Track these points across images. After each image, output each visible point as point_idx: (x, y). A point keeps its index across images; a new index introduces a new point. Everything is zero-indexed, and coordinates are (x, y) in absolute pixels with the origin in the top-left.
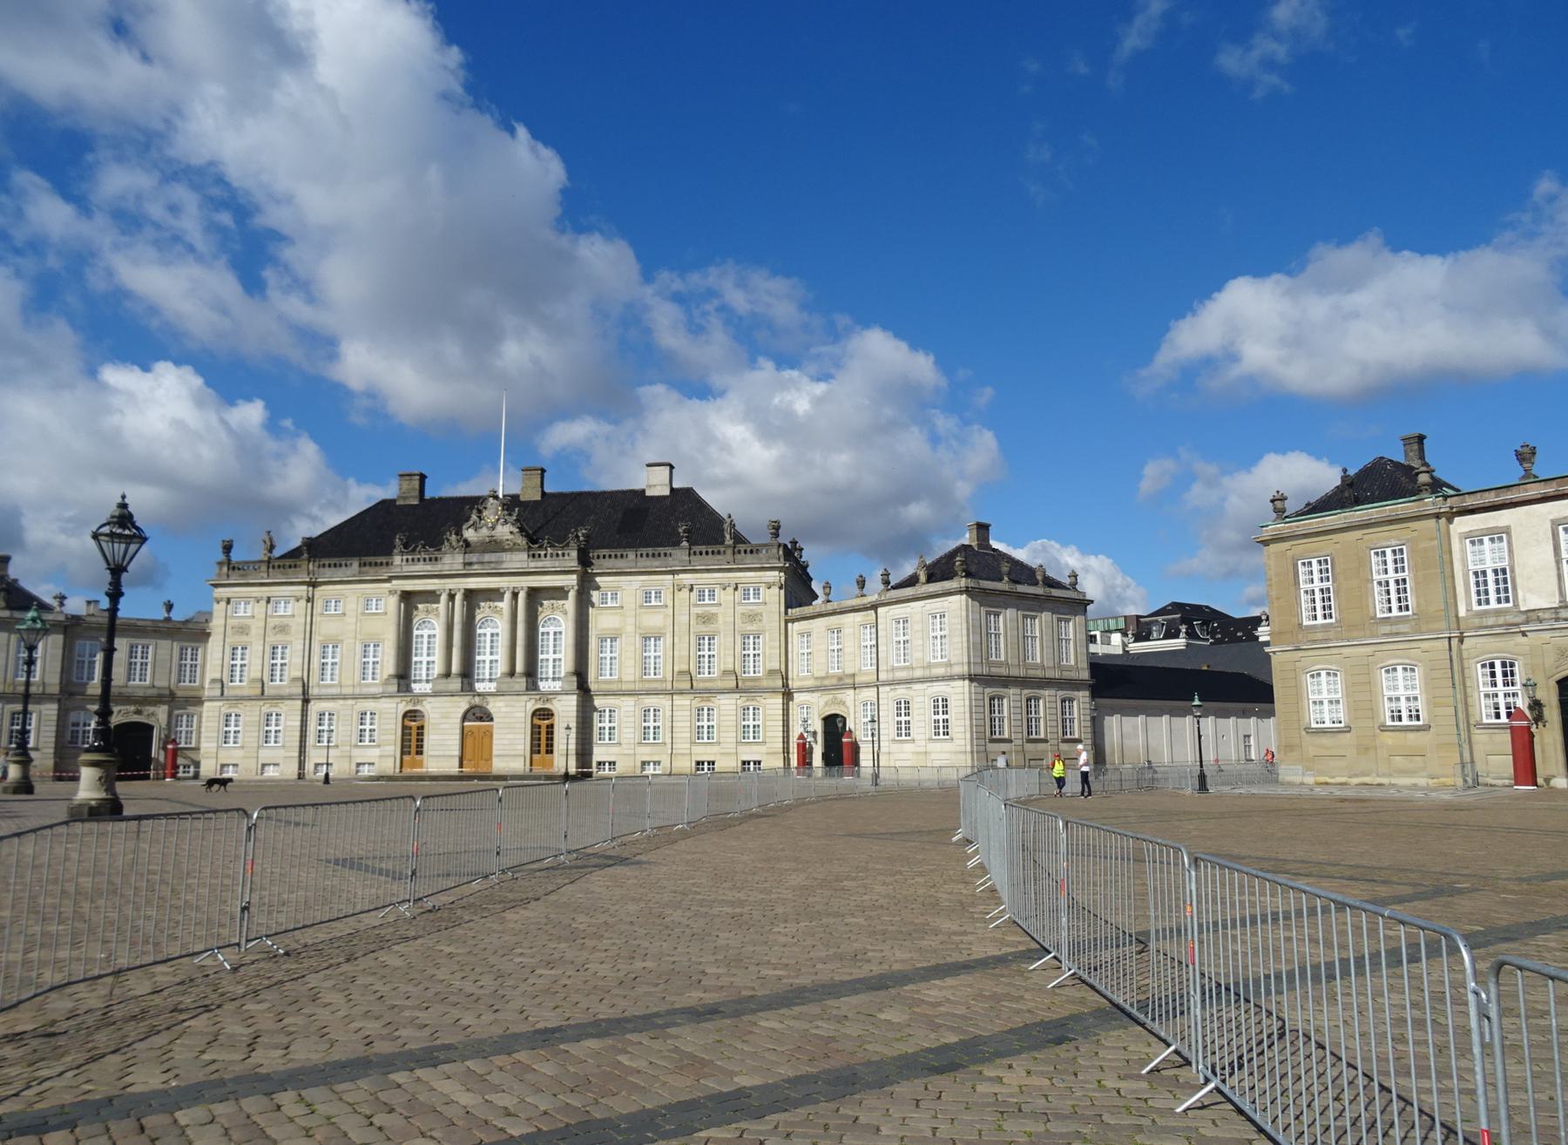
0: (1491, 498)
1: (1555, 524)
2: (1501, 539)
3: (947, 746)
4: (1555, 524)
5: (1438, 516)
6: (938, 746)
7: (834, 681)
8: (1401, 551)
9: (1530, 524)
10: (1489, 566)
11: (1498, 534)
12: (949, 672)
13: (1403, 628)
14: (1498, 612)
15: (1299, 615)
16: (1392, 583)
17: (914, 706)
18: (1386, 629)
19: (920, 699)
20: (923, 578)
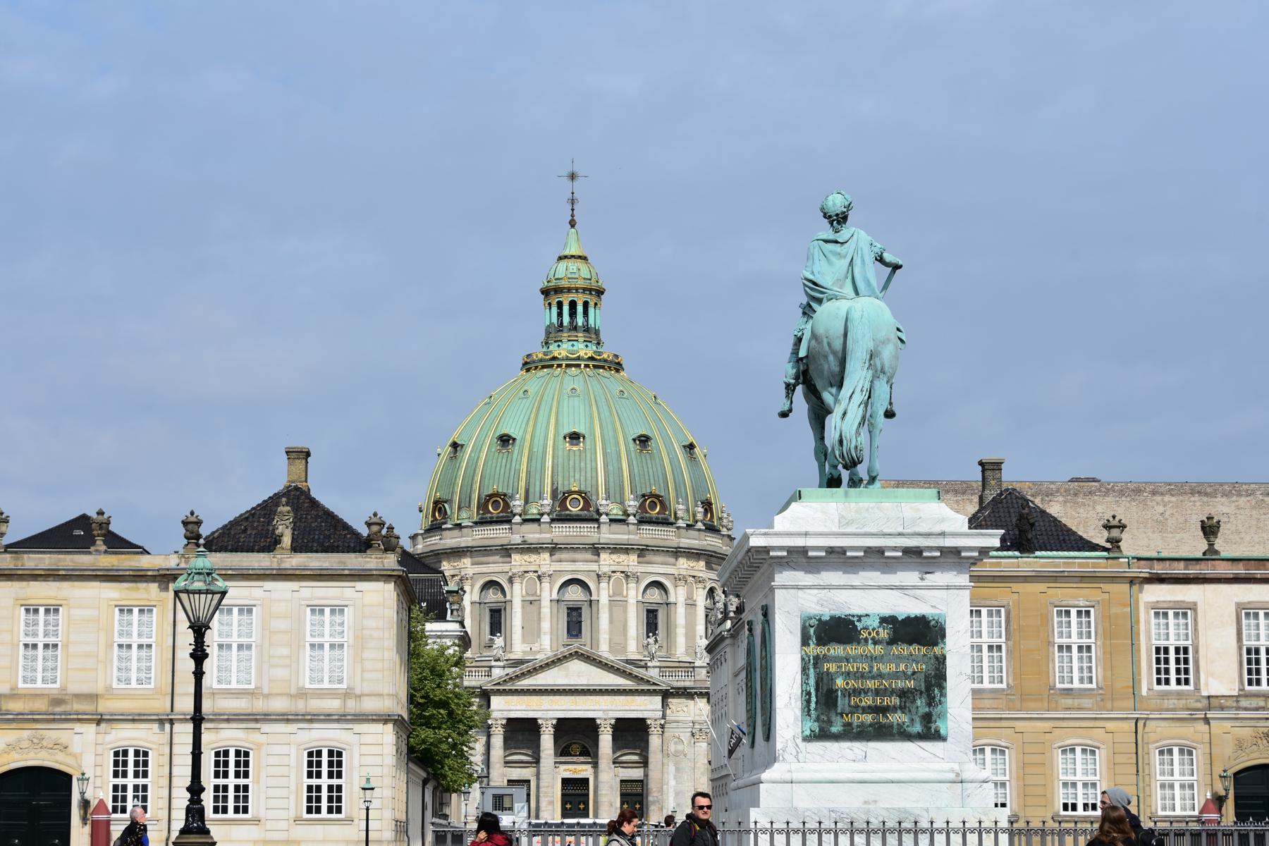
0: (1179, 569)
1: (1240, 607)
2: (1185, 615)
3: (336, 831)
4: (1240, 607)
5: (1132, 581)
6: (317, 831)
7: (41, 705)
8: (1088, 613)
9: (1217, 603)
10: (1172, 643)
11: (1185, 610)
12: (352, 706)
13: (1086, 702)
14: (1179, 695)
16: (1075, 648)
18: (1069, 702)
20: (287, 541)
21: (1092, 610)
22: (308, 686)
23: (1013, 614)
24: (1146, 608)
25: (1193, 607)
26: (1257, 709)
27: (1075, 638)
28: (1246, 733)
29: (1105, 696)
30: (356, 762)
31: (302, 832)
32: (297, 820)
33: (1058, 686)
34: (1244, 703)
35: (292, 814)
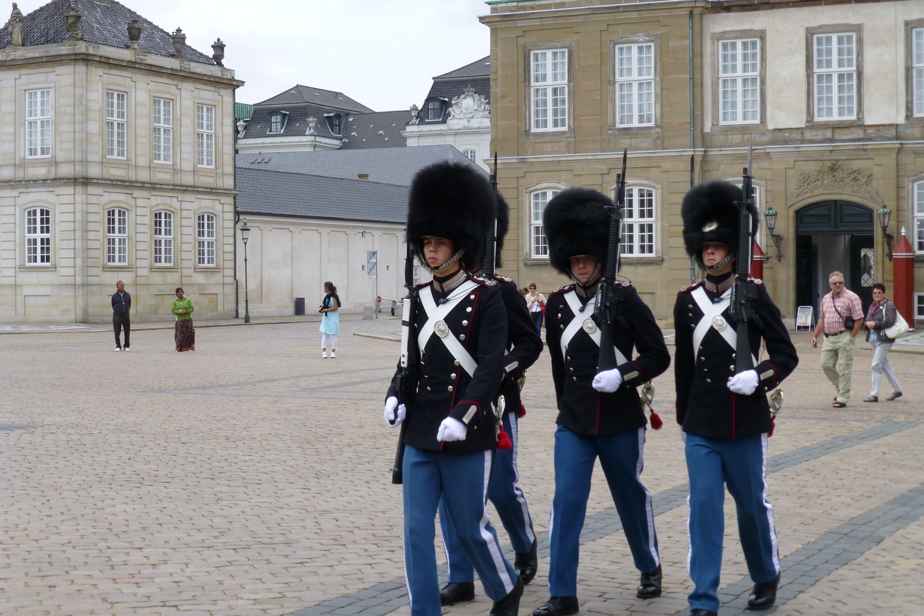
2: (754, 44)
3: (45, 277)
4: (810, 33)
6: (33, 277)
13: (643, 142)
15: (525, 119)
17: (56, 218)
19: (10, 210)
20: (17, 37)
21: (652, 44)
22: (28, 157)
23: (575, 54)
24: (712, 39)
25: (762, 35)
26: (822, 141)
27: (635, 75)
28: (811, 168)
29: (661, 135)
30: (57, 221)
31: (23, 278)
32: (23, 268)
33: (618, 126)
34: (808, 135)
35: (18, 264)
